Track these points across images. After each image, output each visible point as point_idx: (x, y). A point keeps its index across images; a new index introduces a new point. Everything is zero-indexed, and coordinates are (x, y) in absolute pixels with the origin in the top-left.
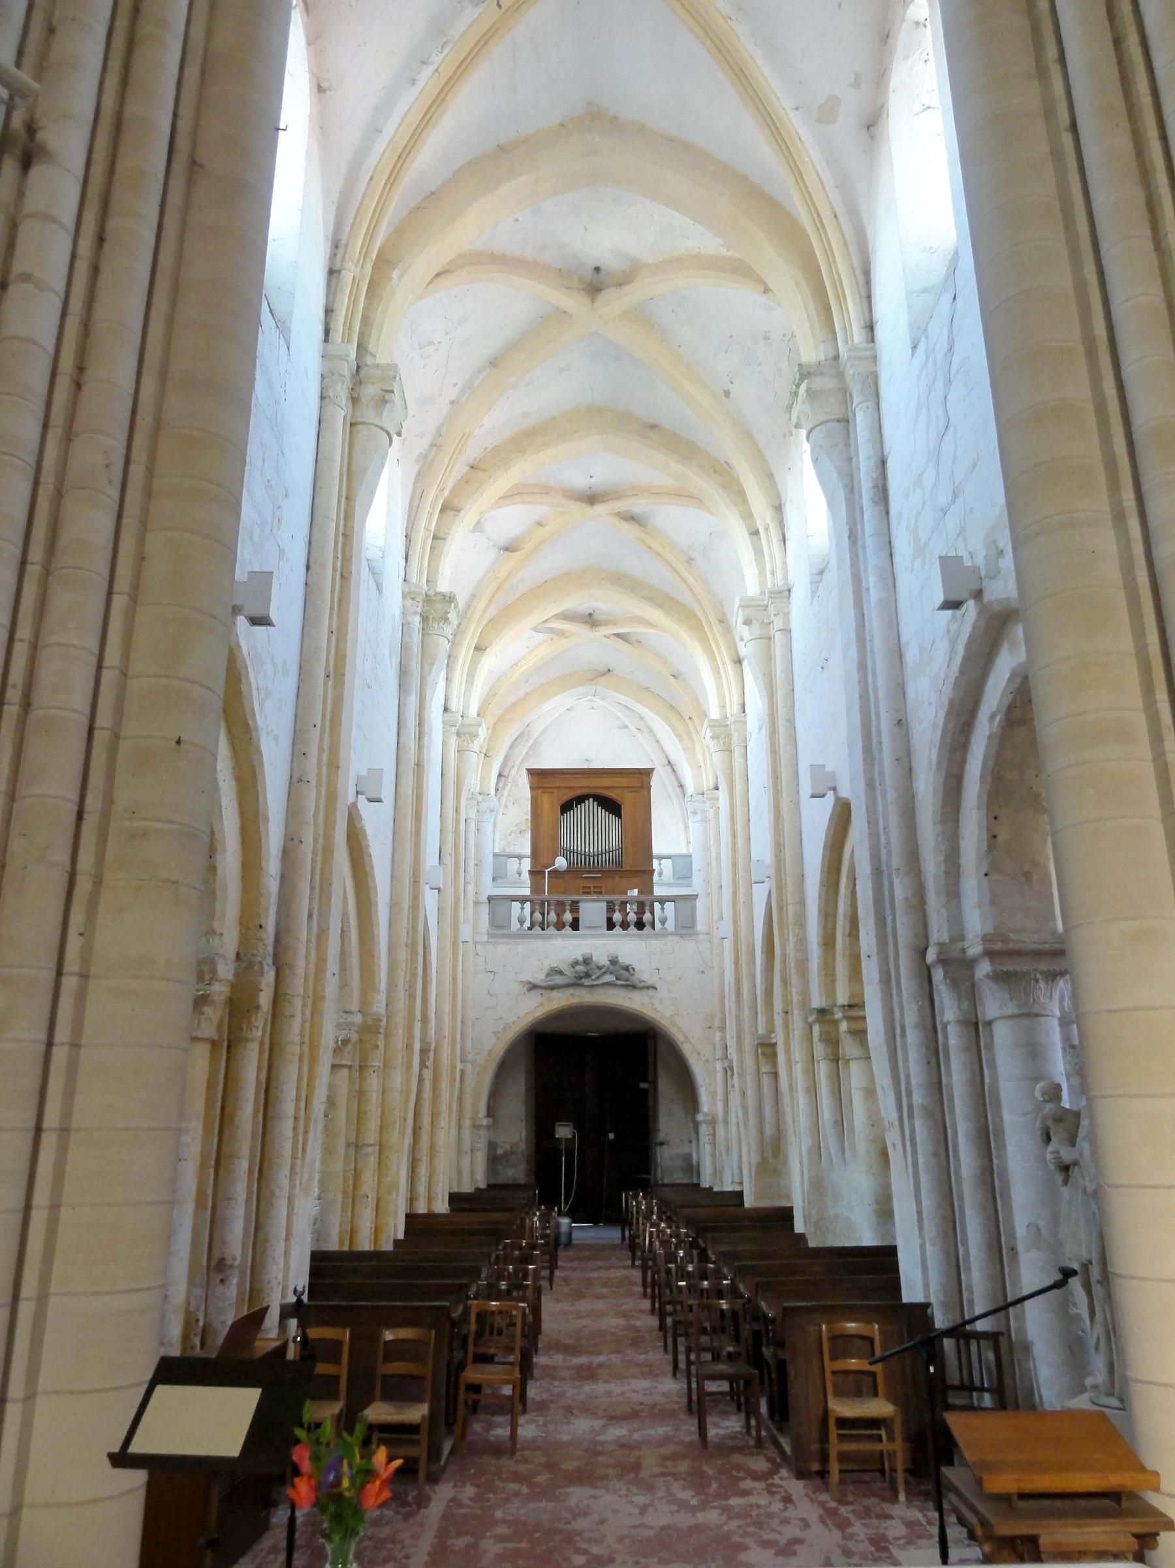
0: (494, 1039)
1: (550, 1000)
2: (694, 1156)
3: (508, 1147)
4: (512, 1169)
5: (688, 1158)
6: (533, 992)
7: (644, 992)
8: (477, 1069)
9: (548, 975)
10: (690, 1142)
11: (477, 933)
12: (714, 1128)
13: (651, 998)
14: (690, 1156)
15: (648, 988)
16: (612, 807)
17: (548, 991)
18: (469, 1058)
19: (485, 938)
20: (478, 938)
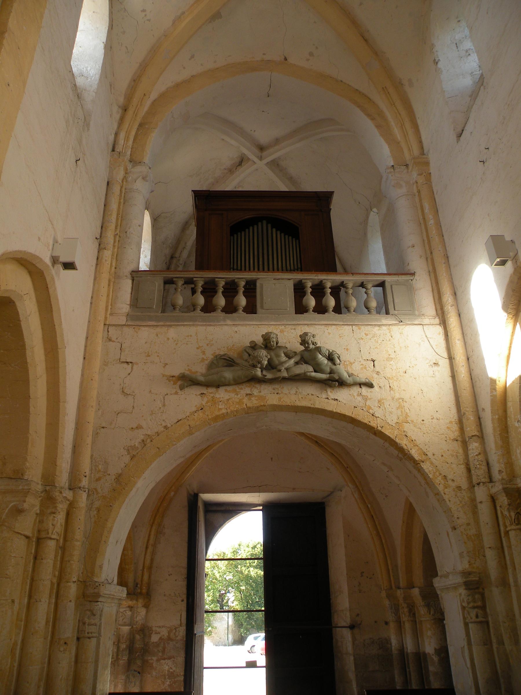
0: (127, 459)
1: (214, 401)
2: (394, 642)
3: (164, 633)
4: (170, 662)
5: (384, 644)
6: (188, 390)
7: (355, 390)
8: (97, 504)
9: (211, 366)
10: (387, 623)
11: (111, 314)
12: (483, 595)
13: (366, 399)
14: (388, 641)
15: (360, 385)
16: (289, 229)
17: (211, 390)
18: (85, 483)
19: (123, 320)
20: (111, 320)
